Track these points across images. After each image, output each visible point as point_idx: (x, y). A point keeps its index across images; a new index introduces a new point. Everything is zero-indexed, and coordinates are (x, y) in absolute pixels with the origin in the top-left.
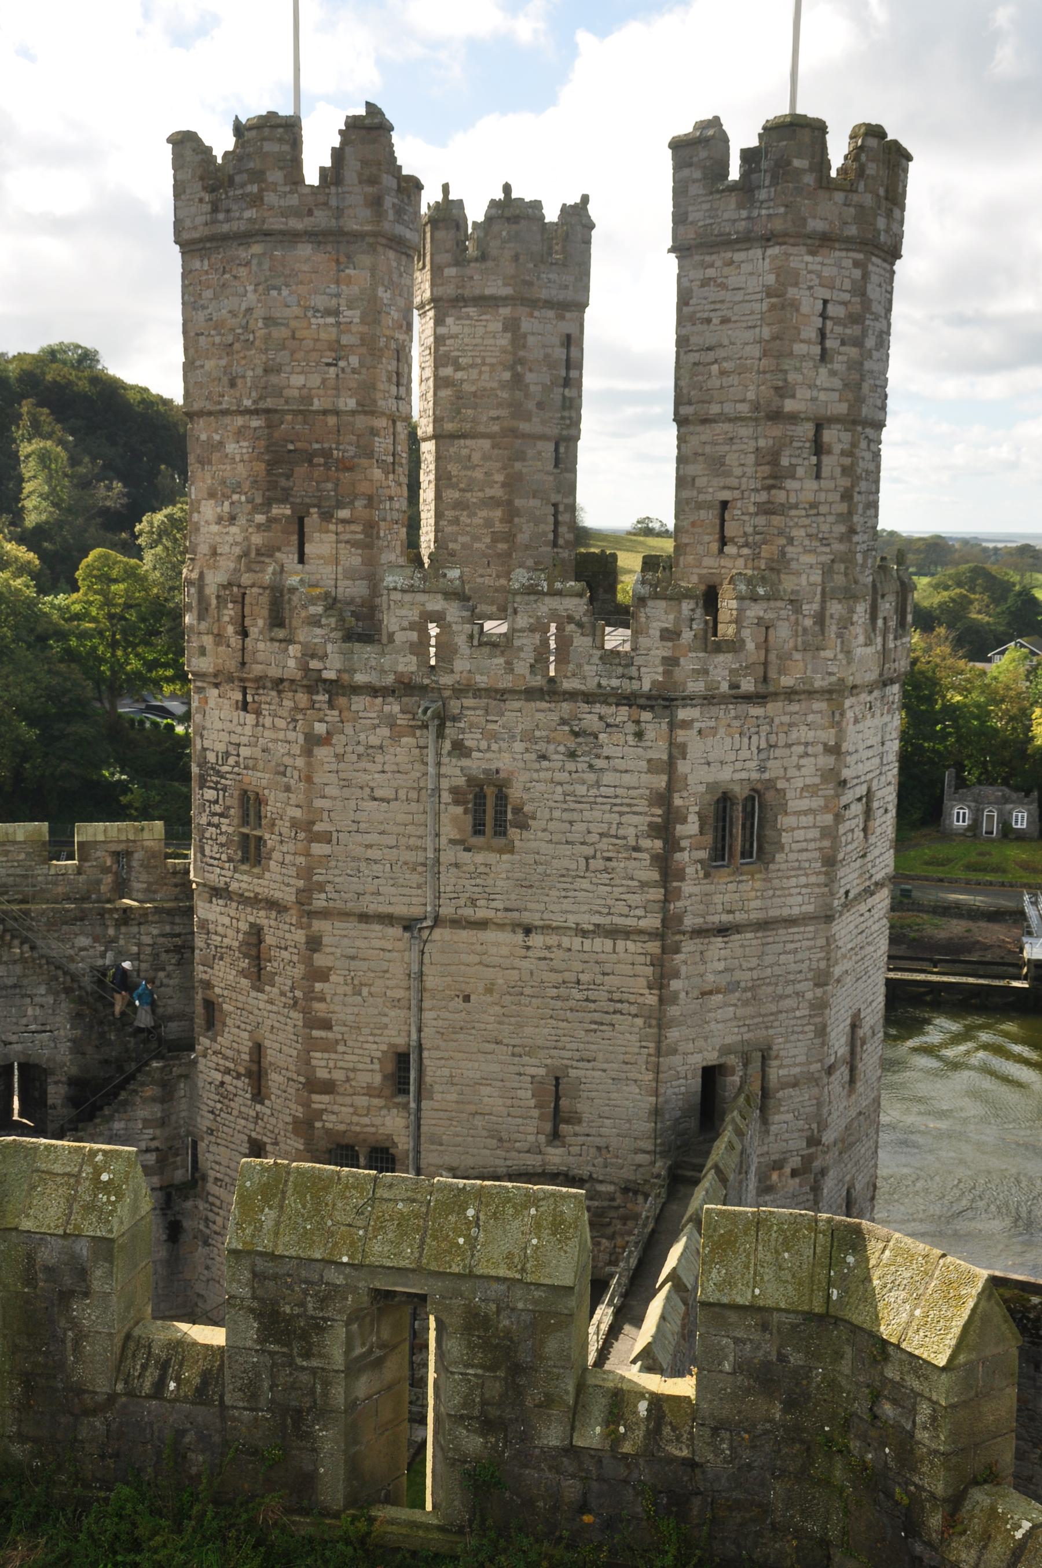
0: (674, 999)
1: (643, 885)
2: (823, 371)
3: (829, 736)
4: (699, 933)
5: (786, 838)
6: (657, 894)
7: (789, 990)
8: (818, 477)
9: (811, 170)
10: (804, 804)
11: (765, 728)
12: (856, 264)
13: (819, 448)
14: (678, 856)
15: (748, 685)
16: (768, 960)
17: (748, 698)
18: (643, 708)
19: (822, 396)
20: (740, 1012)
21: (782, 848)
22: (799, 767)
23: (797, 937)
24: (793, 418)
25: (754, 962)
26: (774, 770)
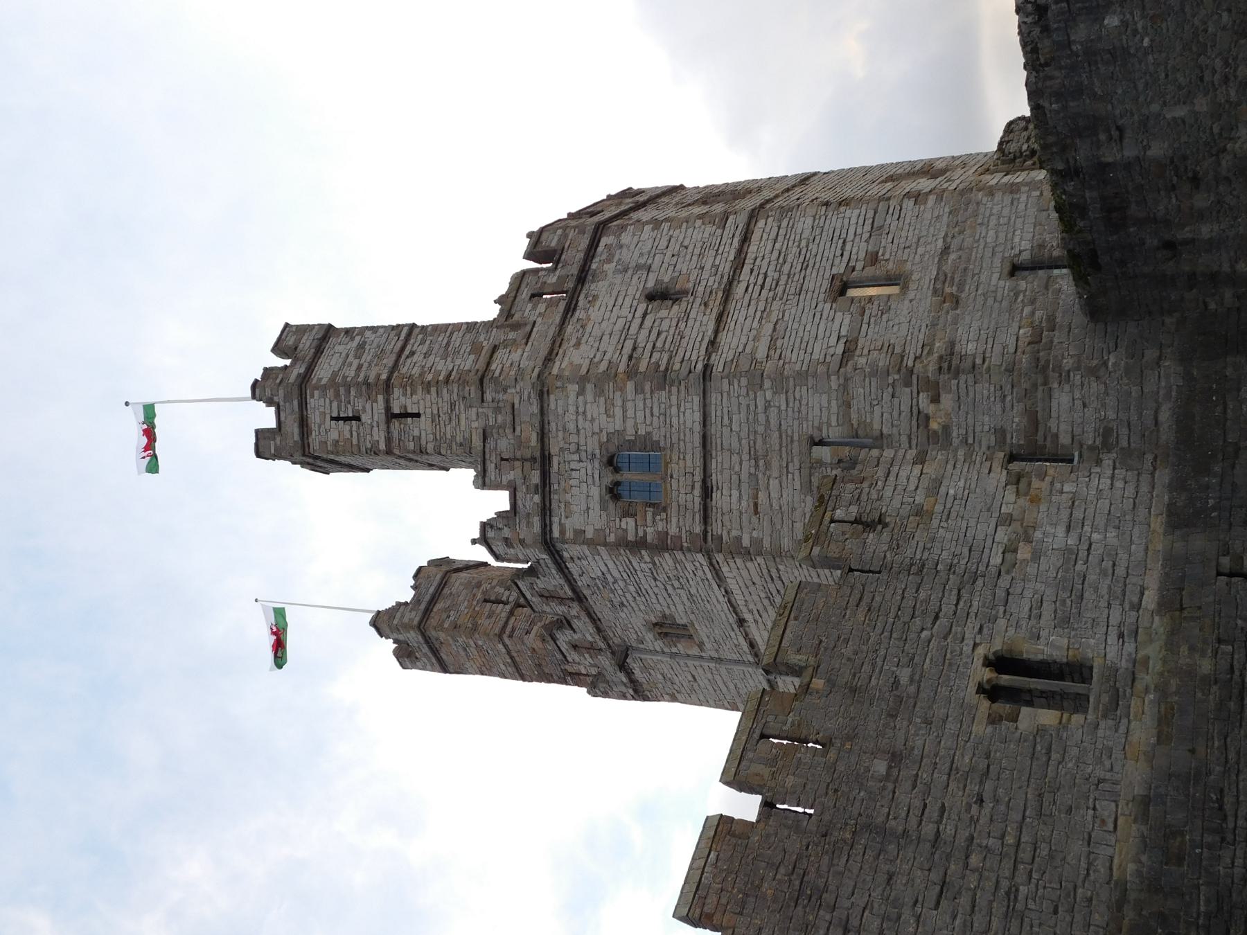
0: (757, 543)
1: (676, 561)
2: (364, 418)
3: (573, 388)
4: (706, 519)
5: (642, 432)
6: (679, 555)
7: (762, 418)
8: (418, 415)
9: (274, 439)
10: (618, 412)
11: (568, 457)
12: (312, 396)
13: (405, 415)
14: (649, 539)
15: (535, 477)
16: (735, 445)
17: (545, 475)
18: (561, 557)
19: (376, 418)
20: (775, 473)
21: (649, 434)
22: (593, 420)
23: (719, 413)
24: (389, 440)
25: (735, 458)
26: (592, 445)
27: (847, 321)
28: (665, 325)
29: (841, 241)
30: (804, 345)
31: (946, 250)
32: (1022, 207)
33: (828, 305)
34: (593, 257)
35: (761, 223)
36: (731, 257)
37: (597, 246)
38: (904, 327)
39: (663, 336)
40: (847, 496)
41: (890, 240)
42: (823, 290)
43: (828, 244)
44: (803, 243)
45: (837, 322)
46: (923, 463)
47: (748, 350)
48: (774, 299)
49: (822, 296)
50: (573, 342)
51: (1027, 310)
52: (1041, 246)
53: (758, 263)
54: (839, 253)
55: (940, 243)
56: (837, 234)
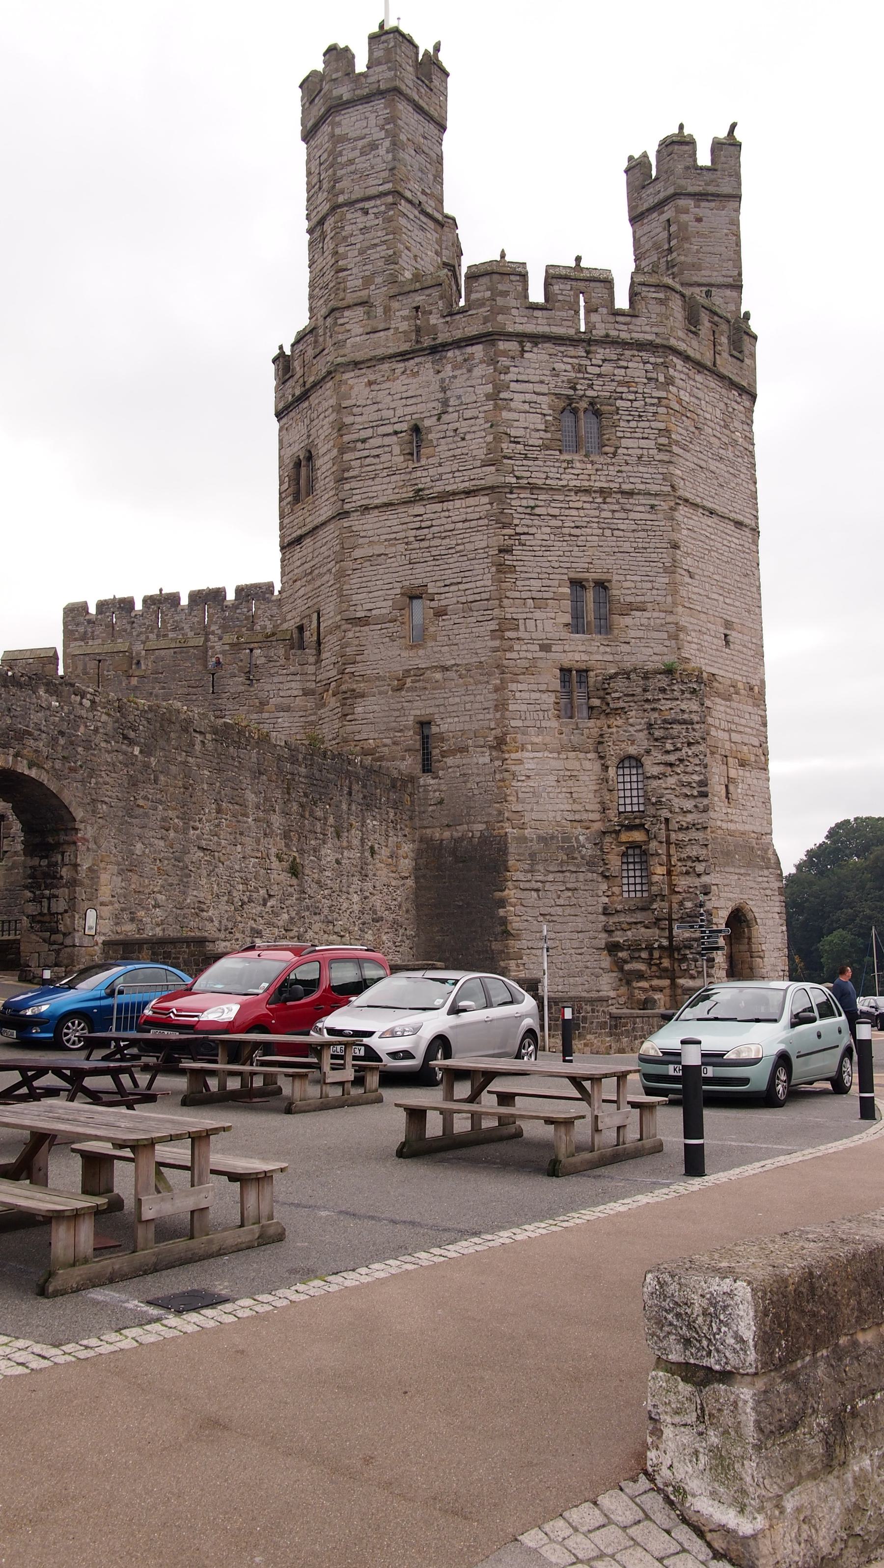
27: (384, 611)
28: (386, 457)
29: (459, 580)
30: (364, 585)
31: (445, 669)
32: (481, 717)
33: (398, 591)
34: (459, 347)
35: (486, 500)
36: (448, 488)
37: (472, 345)
38: (379, 657)
39: (377, 460)
40: (272, 652)
41: (457, 621)
42: (412, 582)
43: (458, 570)
44: (459, 548)
45: (384, 604)
46: (304, 695)
47: (361, 541)
48: (407, 544)
49: (407, 583)
50: (372, 378)
51: (388, 741)
52: (443, 740)
53: (443, 514)
54: (447, 582)
55: (449, 663)
56: (467, 574)
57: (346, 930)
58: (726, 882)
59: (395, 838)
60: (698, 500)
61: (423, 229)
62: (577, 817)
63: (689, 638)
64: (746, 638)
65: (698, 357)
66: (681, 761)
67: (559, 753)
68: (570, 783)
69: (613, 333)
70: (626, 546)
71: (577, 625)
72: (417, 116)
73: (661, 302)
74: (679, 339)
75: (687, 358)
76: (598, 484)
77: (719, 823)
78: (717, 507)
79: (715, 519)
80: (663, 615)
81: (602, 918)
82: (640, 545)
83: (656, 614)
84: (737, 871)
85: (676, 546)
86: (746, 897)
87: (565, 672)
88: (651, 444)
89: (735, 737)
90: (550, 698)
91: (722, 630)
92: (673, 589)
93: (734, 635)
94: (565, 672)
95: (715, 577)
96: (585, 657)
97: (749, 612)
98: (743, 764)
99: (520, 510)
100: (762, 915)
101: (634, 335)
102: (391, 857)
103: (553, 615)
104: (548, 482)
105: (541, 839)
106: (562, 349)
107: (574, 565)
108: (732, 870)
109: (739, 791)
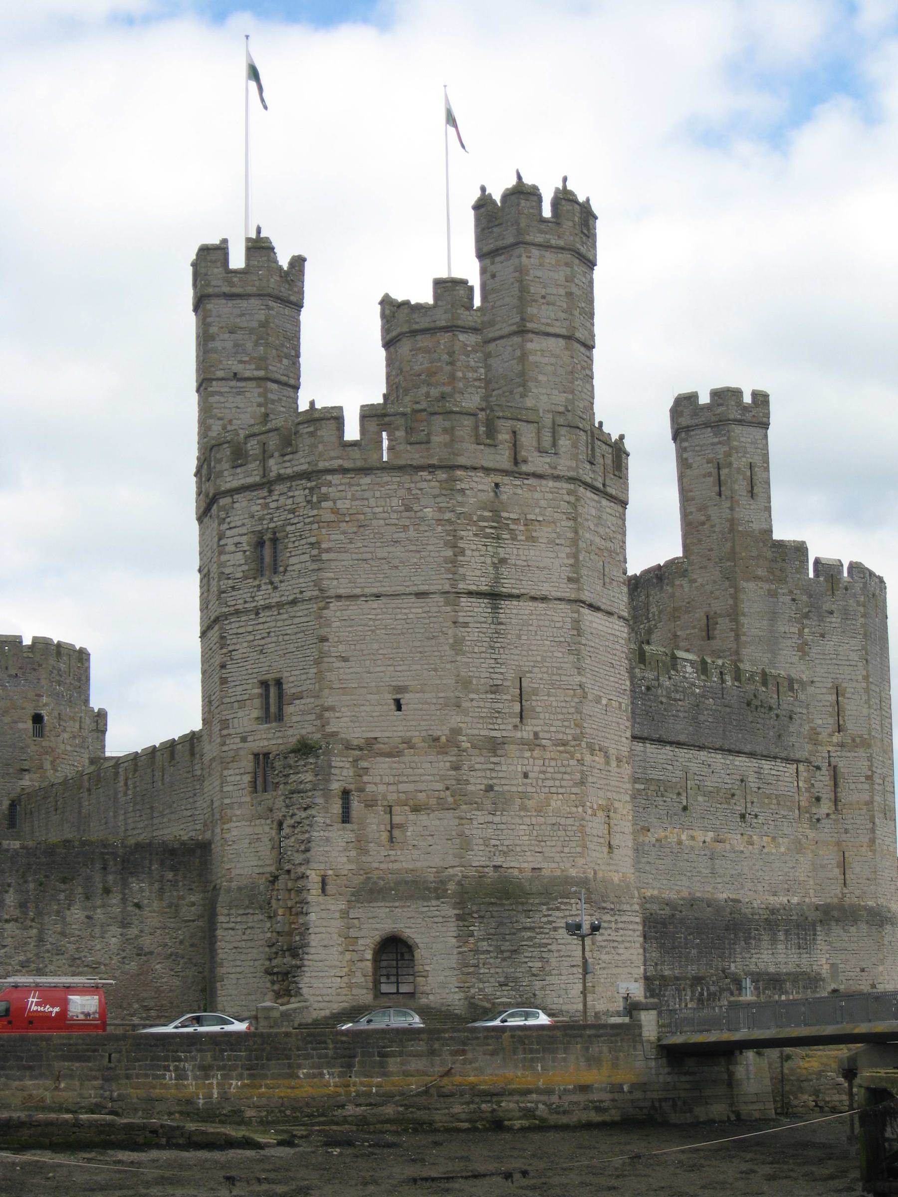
57: (100, 963)
58: (370, 915)
59: (175, 894)
60: (358, 591)
61: (239, 393)
62: (261, 870)
63: (337, 715)
64: (427, 696)
65: (359, 464)
66: (299, 823)
67: (251, 821)
68: (257, 844)
69: (282, 471)
70: (292, 648)
71: (266, 718)
72: (230, 303)
73: (312, 434)
74: (332, 458)
75: (344, 471)
76: (275, 600)
77: (376, 865)
78: (380, 589)
79: (384, 600)
80: (312, 700)
81: (267, 949)
82: (299, 644)
83: (308, 700)
84: (387, 904)
85: (324, 639)
86: (402, 925)
87: (256, 756)
88: (306, 557)
89: (402, 787)
90: (247, 778)
91: (390, 696)
92: (320, 677)
93: (405, 698)
94: (256, 756)
95: (381, 652)
96: (266, 743)
97: (436, 670)
98: (416, 809)
99: (231, 632)
100: (427, 940)
101: (295, 469)
102: (170, 906)
103: (247, 712)
104: (246, 606)
105: (240, 889)
106: (255, 493)
107: (261, 670)
108: (382, 904)
109: (409, 834)
